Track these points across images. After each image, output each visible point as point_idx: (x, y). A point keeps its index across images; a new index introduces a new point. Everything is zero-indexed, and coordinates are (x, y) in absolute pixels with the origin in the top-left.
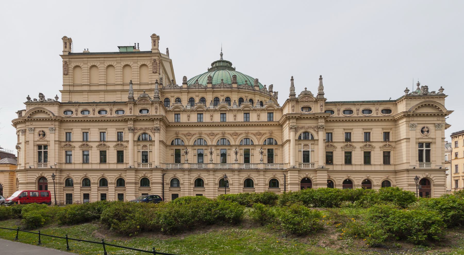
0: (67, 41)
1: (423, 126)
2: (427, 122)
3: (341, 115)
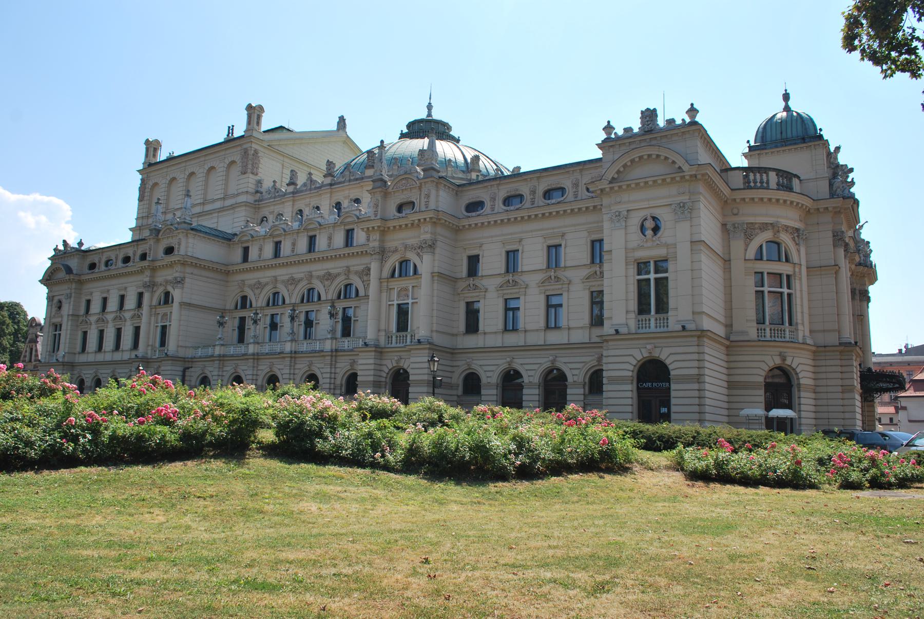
1: (642, 214)
2: (652, 203)
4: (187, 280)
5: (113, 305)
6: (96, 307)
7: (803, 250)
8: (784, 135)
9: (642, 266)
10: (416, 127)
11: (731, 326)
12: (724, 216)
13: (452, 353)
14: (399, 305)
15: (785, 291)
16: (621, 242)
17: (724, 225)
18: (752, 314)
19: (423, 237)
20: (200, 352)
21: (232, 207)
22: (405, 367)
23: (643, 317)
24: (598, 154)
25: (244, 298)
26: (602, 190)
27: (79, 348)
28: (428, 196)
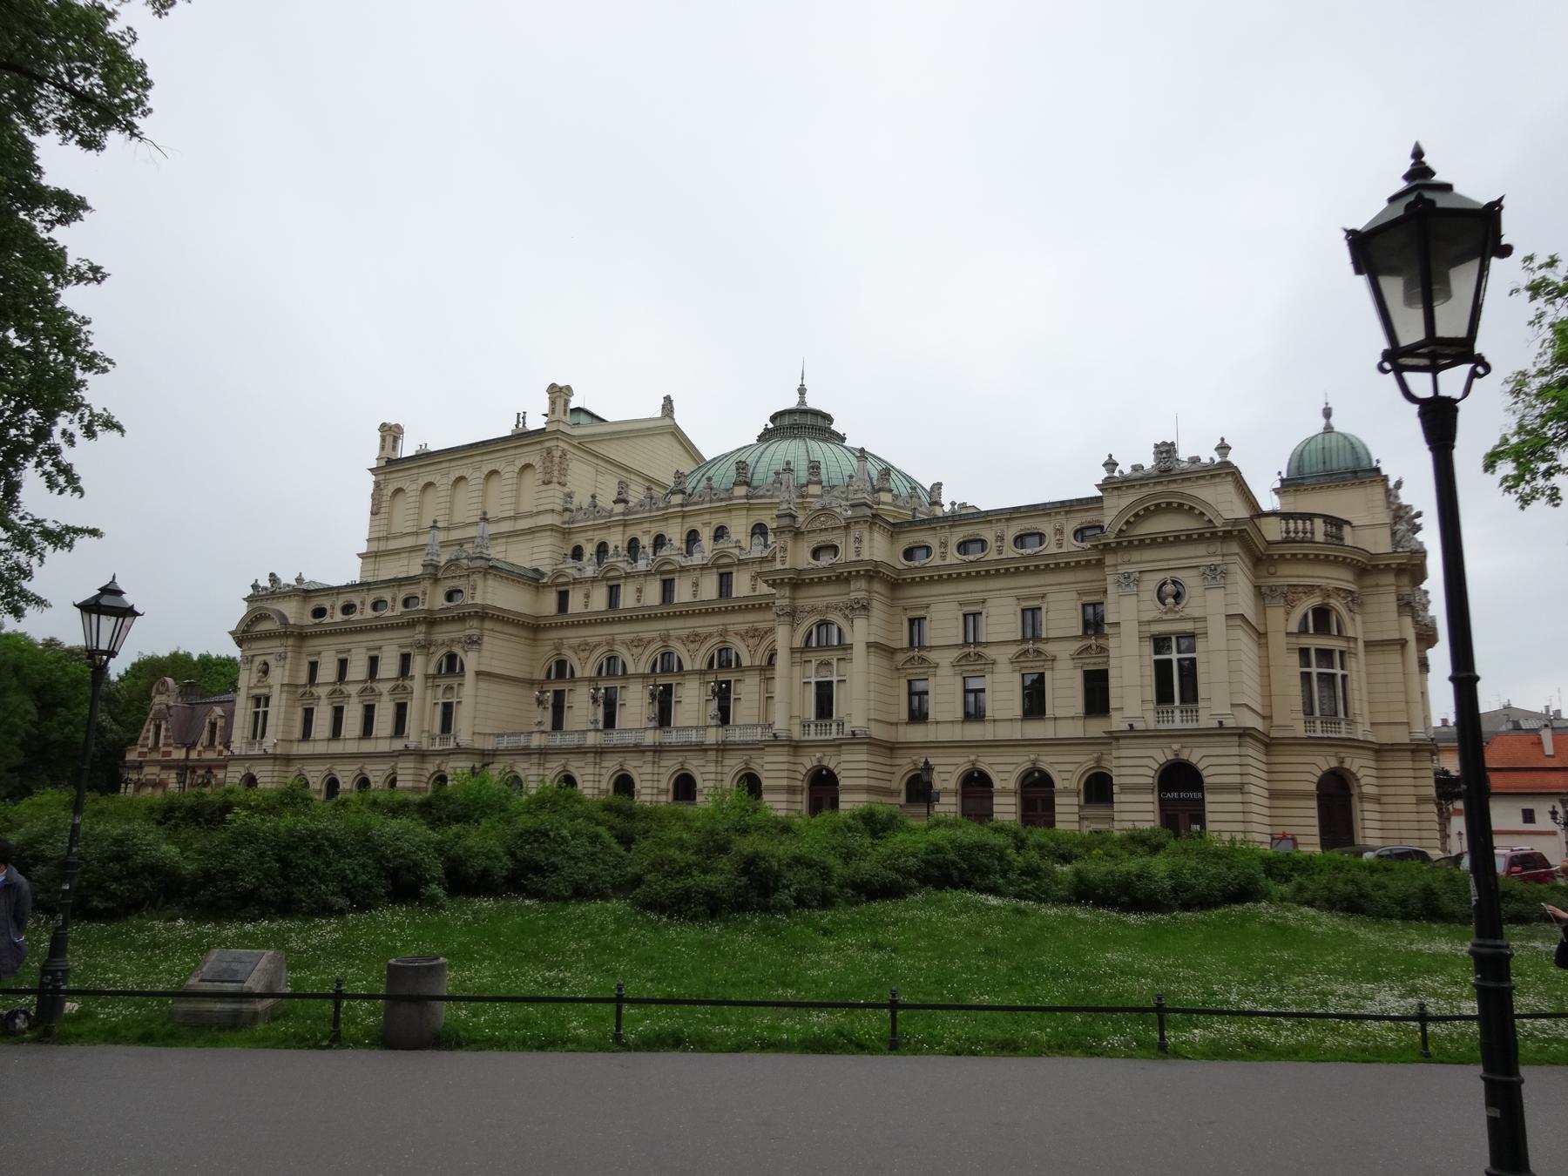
0: (391, 433)
1: (1160, 576)
3: (954, 557)
4: (485, 639)
5: (357, 670)
6: (327, 672)
7: (1358, 618)
8: (1328, 466)
9: (1160, 643)
10: (787, 421)
11: (1270, 717)
12: (1256, 577)
13: (892, 749)
14: (818, 683)
15: (1338, 671)
16: (1131, 612)
17: (1257, 588)
18: (1297, 701)
19: (853, 595)
20: (505, 743)
21: (531, 531)
22: (831, 766)
23: (1166, 707)
24: (1099, 494)
25: (561, 665)
26: (1105, 545)
27: (297, 732)
28: (859, 540)
